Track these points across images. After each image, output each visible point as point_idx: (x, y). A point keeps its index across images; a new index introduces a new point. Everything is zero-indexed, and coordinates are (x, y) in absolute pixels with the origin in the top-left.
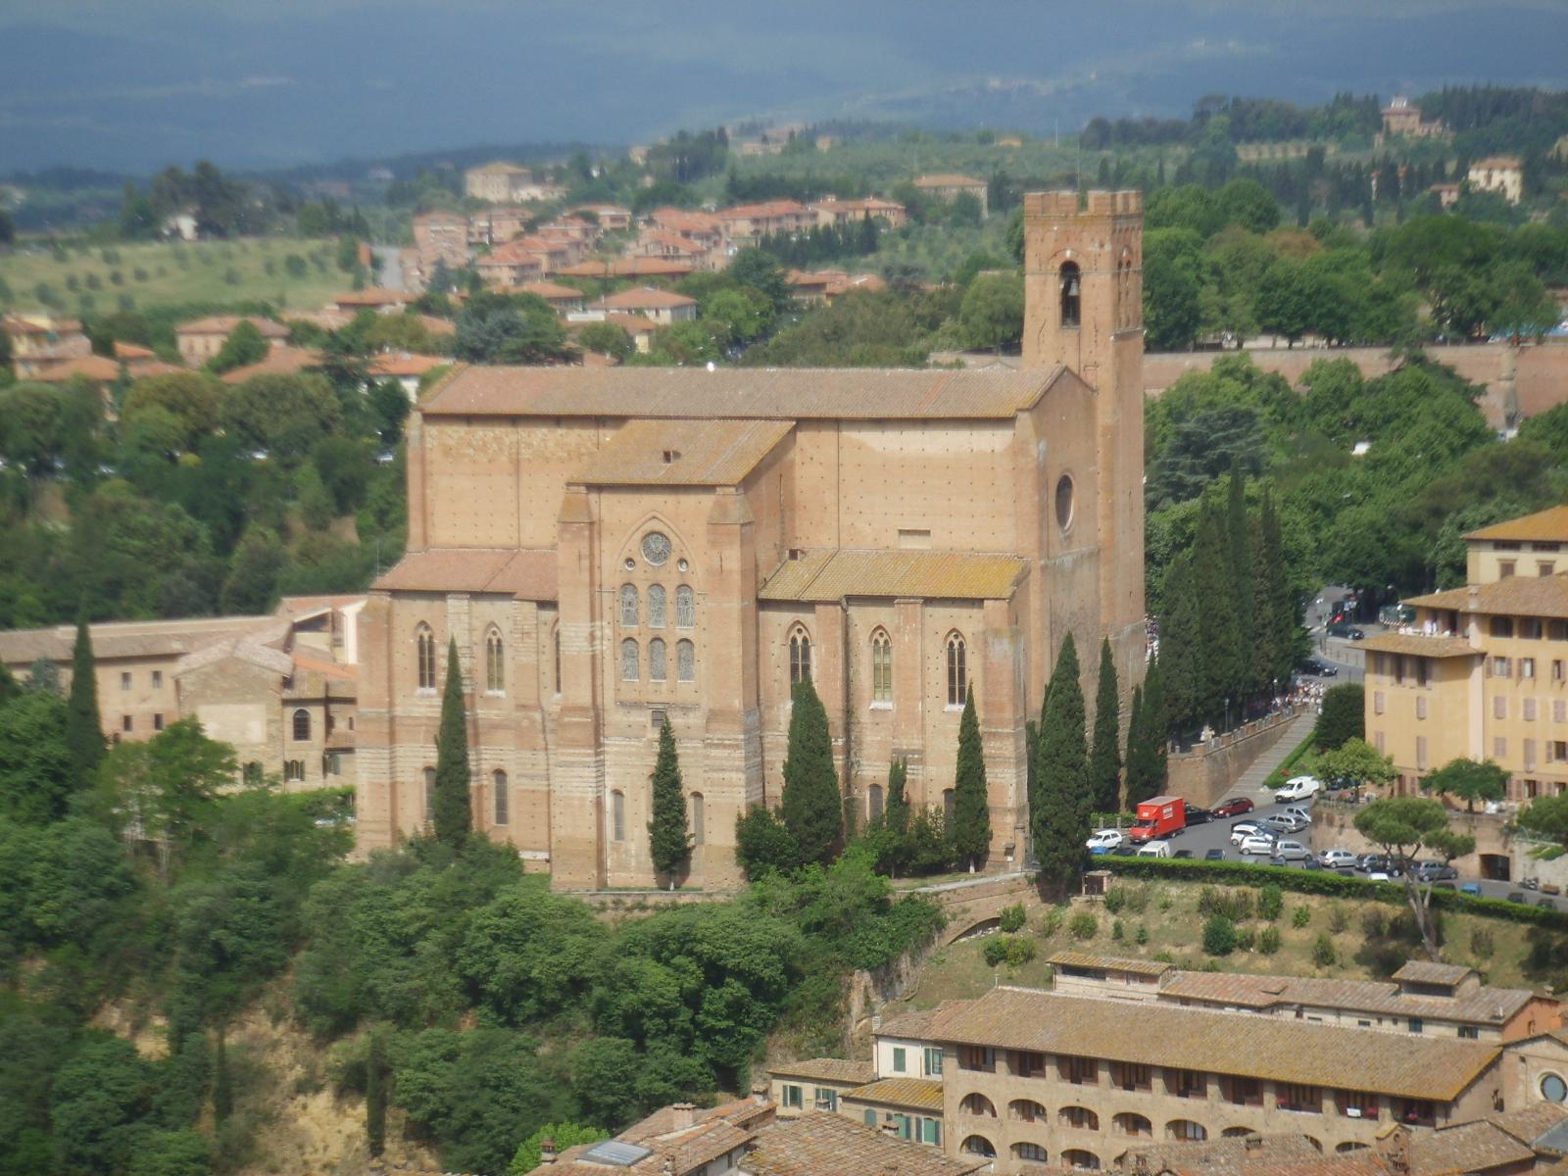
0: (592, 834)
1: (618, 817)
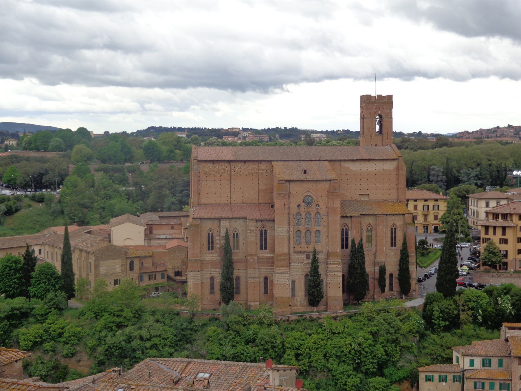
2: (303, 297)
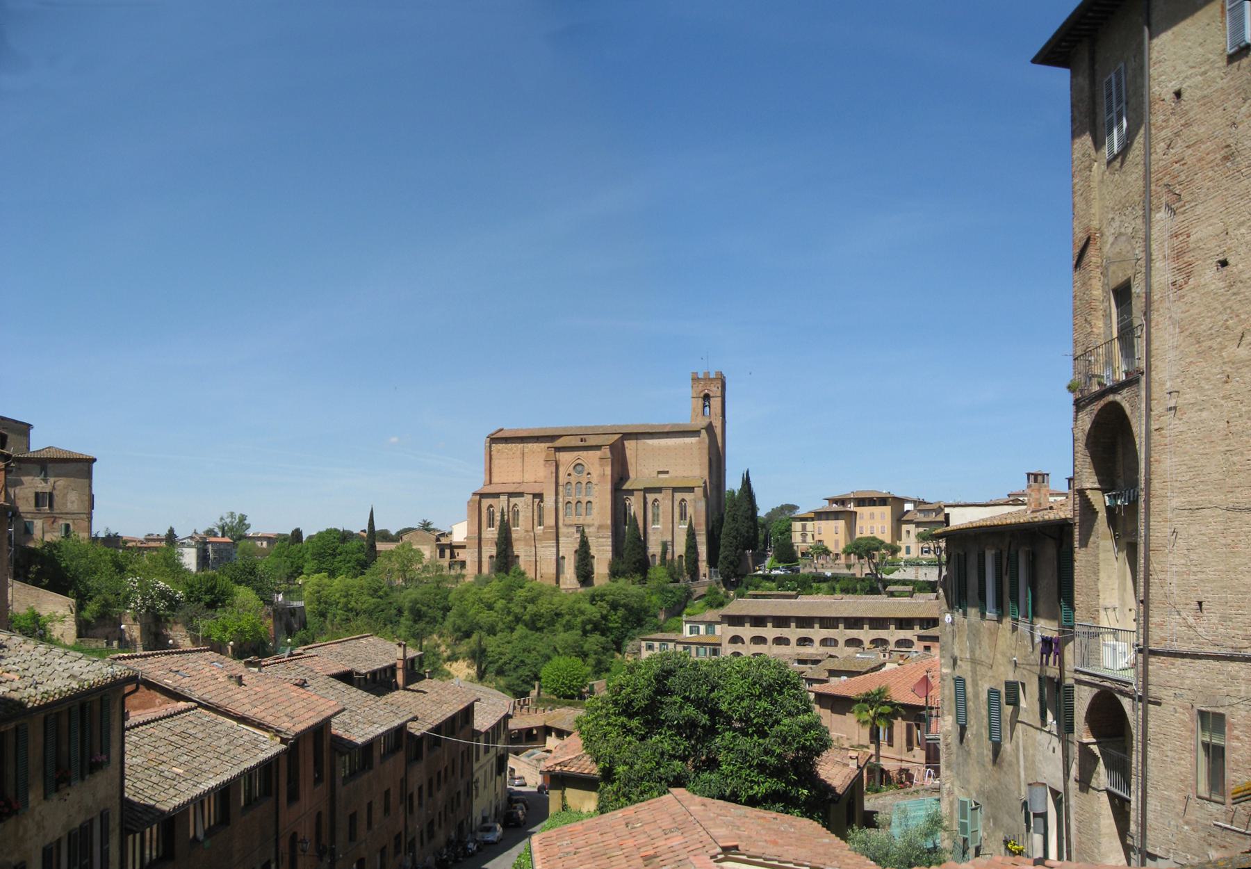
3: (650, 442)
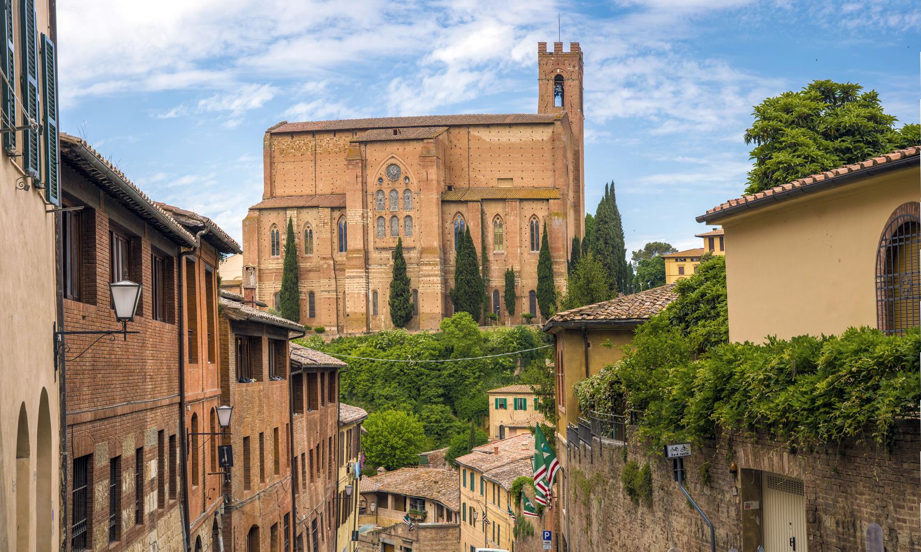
0: (364, 310)
1: (375, 305)
2: (389, 316)
3: (486, 135)
